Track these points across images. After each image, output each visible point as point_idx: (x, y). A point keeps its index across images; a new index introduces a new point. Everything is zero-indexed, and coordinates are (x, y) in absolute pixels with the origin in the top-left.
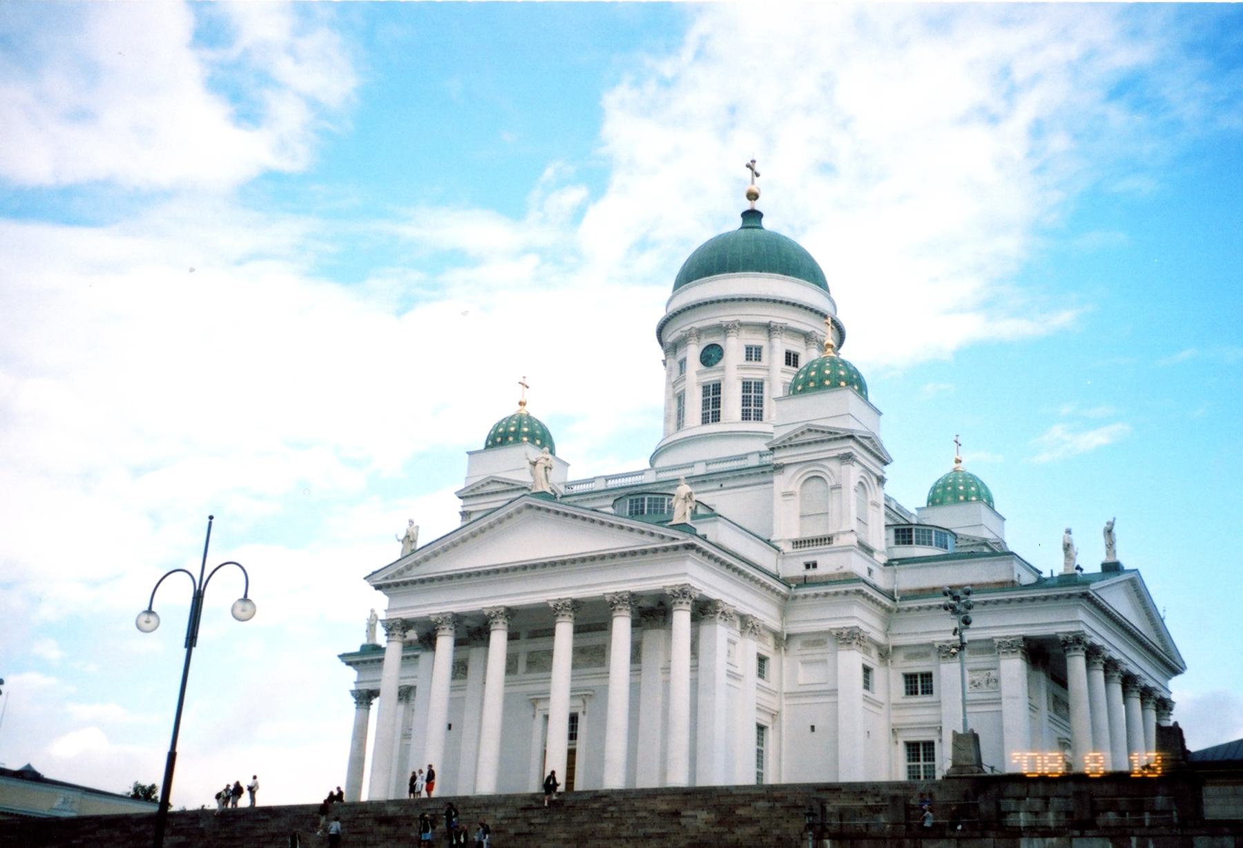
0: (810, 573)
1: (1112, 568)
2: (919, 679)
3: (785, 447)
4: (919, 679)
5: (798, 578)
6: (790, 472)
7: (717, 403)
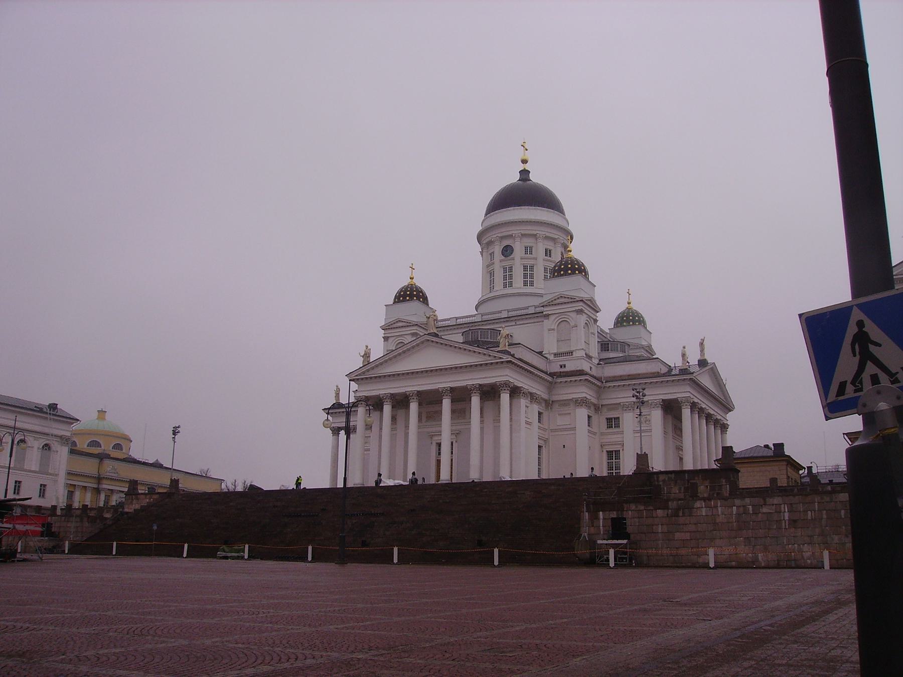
0: (563, 370)
1: (702, 363)
6: (552, 318)
7: (511, 276)
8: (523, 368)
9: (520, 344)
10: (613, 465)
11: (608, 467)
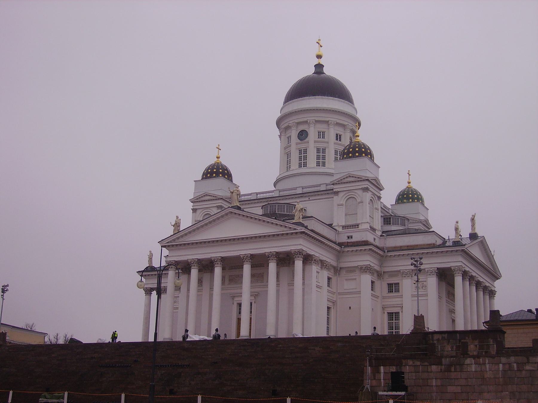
0: (350, 240)
1: (473, 236)
5: (345, 242)
6: (341, 194)
8: (315, 239)
9: (312, 217)
10: (393, 325)
11: (389, 327)
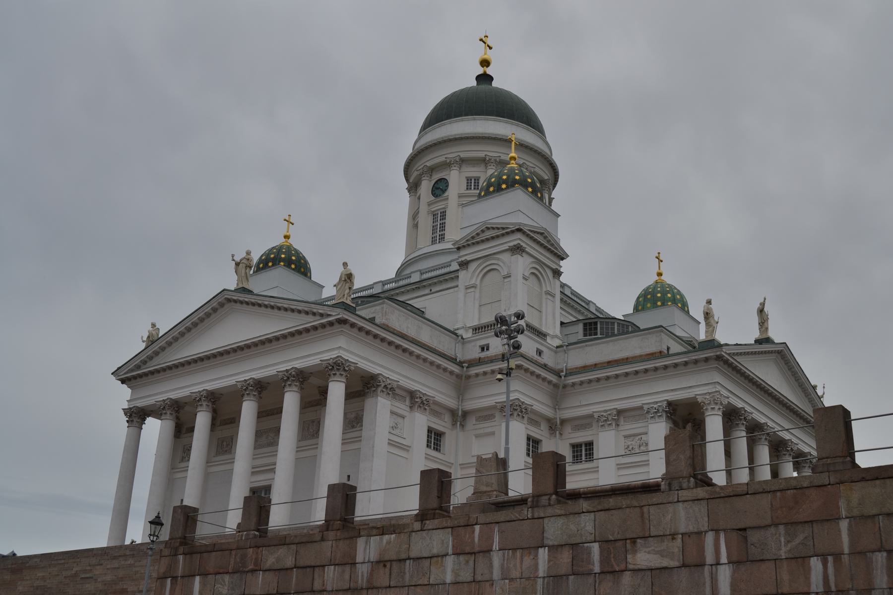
2: (583, 449)
3: (469, 245)
4: (583, 449)
6: (472, 266)
7: (443, 227)
